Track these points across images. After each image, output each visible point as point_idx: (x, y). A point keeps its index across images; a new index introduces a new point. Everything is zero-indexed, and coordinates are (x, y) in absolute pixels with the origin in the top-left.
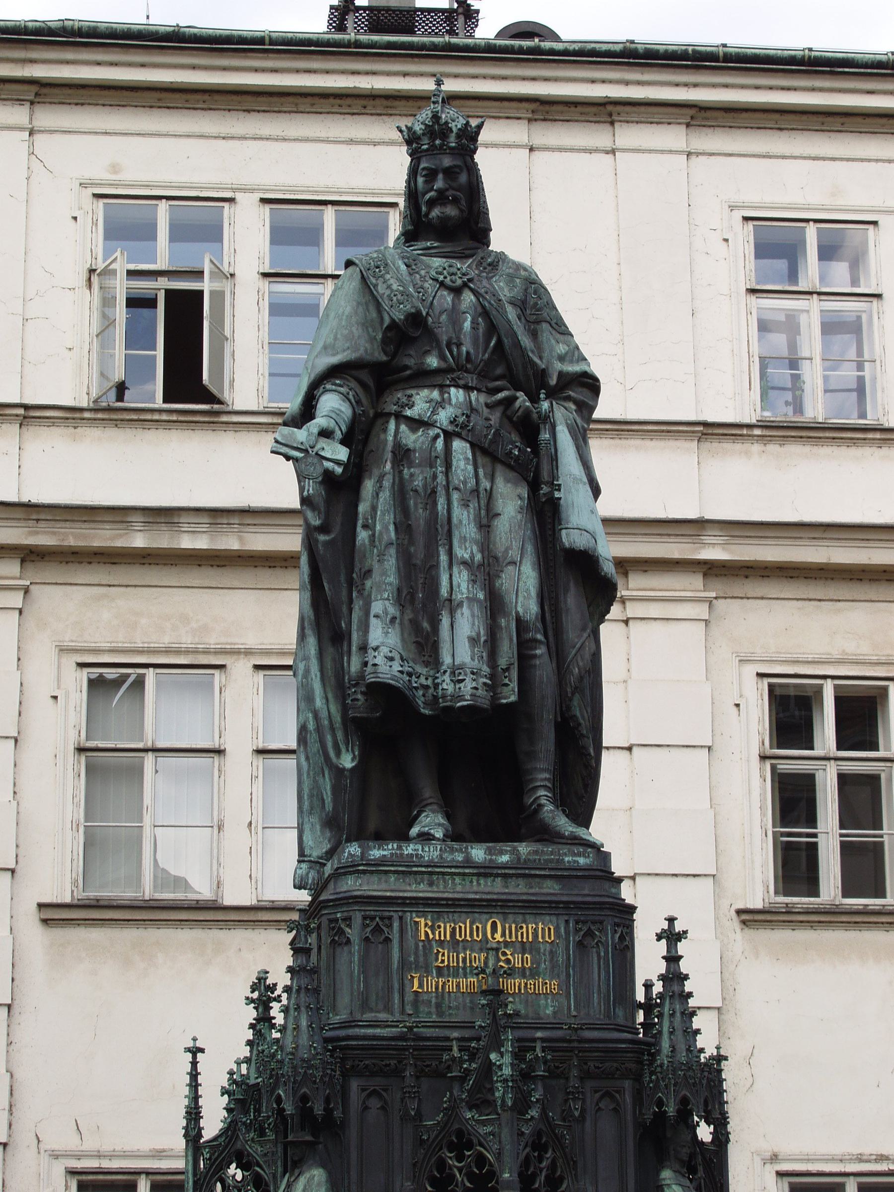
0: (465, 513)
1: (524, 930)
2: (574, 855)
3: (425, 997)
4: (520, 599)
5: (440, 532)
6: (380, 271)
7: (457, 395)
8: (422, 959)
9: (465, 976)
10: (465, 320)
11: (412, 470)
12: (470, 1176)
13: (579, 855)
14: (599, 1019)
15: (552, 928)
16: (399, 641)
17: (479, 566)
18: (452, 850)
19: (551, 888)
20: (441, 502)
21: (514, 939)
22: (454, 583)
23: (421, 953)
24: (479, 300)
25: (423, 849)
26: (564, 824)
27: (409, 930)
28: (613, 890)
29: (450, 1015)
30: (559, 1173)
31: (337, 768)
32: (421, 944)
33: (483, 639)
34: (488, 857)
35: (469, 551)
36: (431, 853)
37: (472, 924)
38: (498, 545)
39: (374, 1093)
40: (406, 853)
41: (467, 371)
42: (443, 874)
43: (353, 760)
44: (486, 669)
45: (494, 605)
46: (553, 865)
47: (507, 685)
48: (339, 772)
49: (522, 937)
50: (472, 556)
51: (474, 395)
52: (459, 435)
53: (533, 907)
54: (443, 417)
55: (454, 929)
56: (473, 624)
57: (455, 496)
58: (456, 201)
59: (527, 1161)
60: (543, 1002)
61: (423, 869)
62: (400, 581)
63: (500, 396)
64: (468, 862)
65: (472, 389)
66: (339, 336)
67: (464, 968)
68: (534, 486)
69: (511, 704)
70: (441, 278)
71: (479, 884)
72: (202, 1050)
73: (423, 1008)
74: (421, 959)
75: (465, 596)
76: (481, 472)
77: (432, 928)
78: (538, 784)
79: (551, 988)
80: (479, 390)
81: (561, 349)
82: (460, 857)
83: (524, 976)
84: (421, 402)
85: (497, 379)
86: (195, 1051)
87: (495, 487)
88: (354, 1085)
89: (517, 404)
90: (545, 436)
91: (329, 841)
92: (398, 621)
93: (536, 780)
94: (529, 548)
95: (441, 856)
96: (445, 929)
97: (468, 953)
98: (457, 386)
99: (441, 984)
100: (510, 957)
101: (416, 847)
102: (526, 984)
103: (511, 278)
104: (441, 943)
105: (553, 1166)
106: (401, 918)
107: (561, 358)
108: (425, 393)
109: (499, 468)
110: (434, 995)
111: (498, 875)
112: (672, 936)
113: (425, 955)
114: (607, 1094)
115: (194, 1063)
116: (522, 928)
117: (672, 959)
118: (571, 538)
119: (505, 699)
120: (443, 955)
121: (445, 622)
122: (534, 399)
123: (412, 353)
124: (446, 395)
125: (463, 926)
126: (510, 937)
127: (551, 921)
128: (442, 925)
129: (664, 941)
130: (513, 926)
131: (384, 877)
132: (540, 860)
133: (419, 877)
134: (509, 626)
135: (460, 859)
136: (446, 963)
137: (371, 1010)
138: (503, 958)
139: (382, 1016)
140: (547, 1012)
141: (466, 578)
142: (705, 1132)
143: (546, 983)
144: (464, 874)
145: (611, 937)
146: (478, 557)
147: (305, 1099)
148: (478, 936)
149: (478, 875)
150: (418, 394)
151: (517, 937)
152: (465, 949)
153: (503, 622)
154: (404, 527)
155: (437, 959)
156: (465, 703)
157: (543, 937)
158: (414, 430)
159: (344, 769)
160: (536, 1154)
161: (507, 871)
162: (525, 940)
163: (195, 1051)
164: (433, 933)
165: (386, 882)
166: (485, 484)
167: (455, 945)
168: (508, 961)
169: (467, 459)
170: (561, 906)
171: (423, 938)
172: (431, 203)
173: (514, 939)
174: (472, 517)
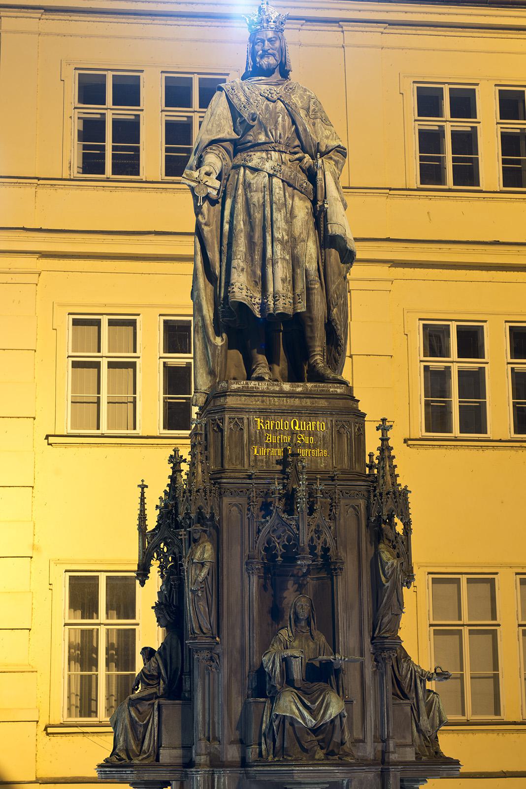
0: (279, 215)
1: (310, 425)
2: (335, 388)
3: (260, 458)
4: (307, 259)
5: (268, 225)
6: (234, 92)
7: (275, 155)
8: (259, 439)
9: (280, 448)
10: (279, 117)
11: (252, 193)
12: (284, 546)
13: (337, 387)
14: (347, 469)
15: (324, 424)
16: (245, 280)
17: (287, 242)
18: (273, 385)
20: (268, 209)
21: (305, 429)
22: (274, 251)
23: (258, 436)
24: (286, 107)
25: (259, 384)
26: (329, 373)
27: (252, 424)
28: (355, 406)
29: (273, 467)
30: (328, 545)
31: (214, 344)
32: (258, 431)
33: (288, 279)
34: (292, 389)
35: (281, 234)
36: (263, 386)
37: (284, 421)
38: (296, 232)
40: (250, 386)
41: (280, 143)
42: (269, 396)
43: (222, 340)
44: (290, 295)
45: (295, 262)
46: (325, 393)
47: (300, 302)
48: (216, 346)
49: (309, 428)
50: (283, 237)
51: (283, 155)
52: (276, 176)
53: (313, 413)
54: (268, 166)
55: (275, 424)
56: (284, 272)
57: (274, 207)
58: (274, 55)
59: (312, 540)
60: (319, 461)
61: (259, 394)
62: (246, 250)
63: (297, 156)
64: (281, 392)
65: (282, 152)
66: (214, 125)
67: (280, 444)
68: (314, 202)
69: (303, 312)
70: (267, 95)
71: (287, 402)
72: (147, 487)
73: (260, 464)
74: (258, 439)
75: (279, 257)
76: (287, 194)
77: (264, 424)
78: (316, 353)
79: (323, 454)
80: (286, 153)
81: (327, 133)
82: (277, 389)
83: (310, 448)
84: (256, 159)
85: (295, 147)
86: (143, 487)
87: (294, 203)
88: (226, 500)
89: (305, 160)
90: (320, 176)
91: (210, 382)
92: (245, 270)
93: (315, 351)
94: (312, 233)
95: (268, 388)
96: (270, 424)
97: (282, 436)
98: (275, 151)
99: (268, 451)
100: (303, 438)
101: (255, 383)
102: (311, 452)
103: (301, 97)
104: (268, 431)
106: (248, 419)
107: (327, 138)
108: (258, 154)
109: (296, 191)
110: (264, 457)
111: (296, 397)
112: (384, 427)
113: (260, 437)
115: (143, 494)
116: (309, 424)
117: (384, 440)
119: (299, 309)
120: (269, 437)
121: (269, 270)
122: (313, 157)
123: (252, 134)
124: (269, 155)
125: (279, 423)
126: (303, 428)
127: (323, 421)
128: (269, 422)
129: (380, 431)
130: (305, 423)
131: (239, 398)
132: (317, 390)
133: (256, 398)
135: (277, 389)
136: (271, 441)
137: (233, 464)
138: (299, 439)
139: (239, 467)
140: (322, 466)
141: (280, 248)
142: (400, 528)
143: (321, 451)
144: (280, 397)
145: (354, 430)
146: (286, 237)
147: (200, 508)
148: (287, 428)
149: (287, 397)
150: (255, 155)
151: (306, 429)
152: (280, 434)
153: (299, 271)
155: (266, 439)
156: (280, 311)
157: (320, 429)
158: (252, 173)
159: (217, 346)
160: (317, 535)
161: (301, 395)
162: (310, 430)
163: (143, 487)
164: (264, 426)
165: (240, 400)
166: (290, 201)
167: (274, 432)
168: (302, 440)
169: (280, 188)
170: (329, 413)
171: (259, 428)
172: (262, 57)
173: (305, 429)
174: (283, 217)
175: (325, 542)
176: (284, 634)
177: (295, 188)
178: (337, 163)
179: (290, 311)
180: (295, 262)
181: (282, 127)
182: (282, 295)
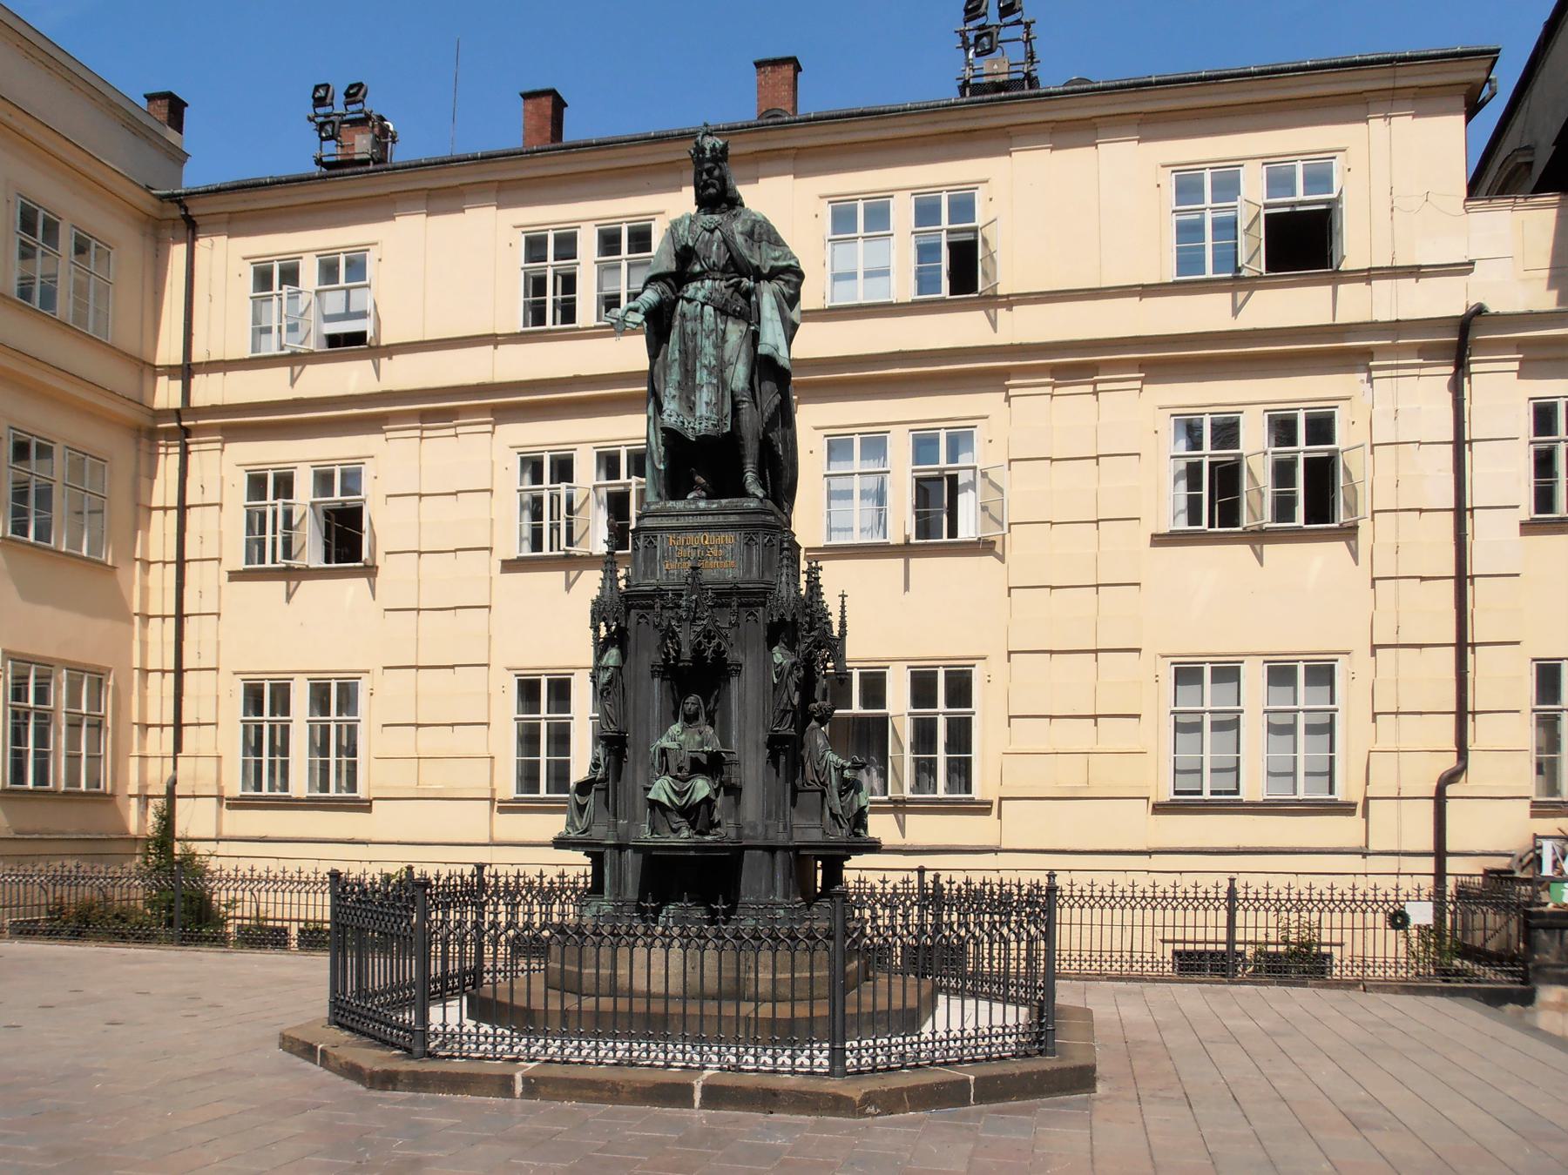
7: (708, 283)
19: (733, 519)
39: (642, 616)
54: (700, 296)
59: (700, 643)
81: (777, 254)
88: (633, 612)
90: (753, 298)
94: (743, 356)
96: (681, 539)
105: (719, 645)
107: (776, 259)
114: (751, 614)
118: (762, 350)
134: (728, 395)
154: (684, 352)
175: (719, 645)
176: (676, 728)
177: (728, 315)
178: (787, 282)
179: (712, 431)
180: (723, 383)
181: (716, 254)
182: (703, 417)
